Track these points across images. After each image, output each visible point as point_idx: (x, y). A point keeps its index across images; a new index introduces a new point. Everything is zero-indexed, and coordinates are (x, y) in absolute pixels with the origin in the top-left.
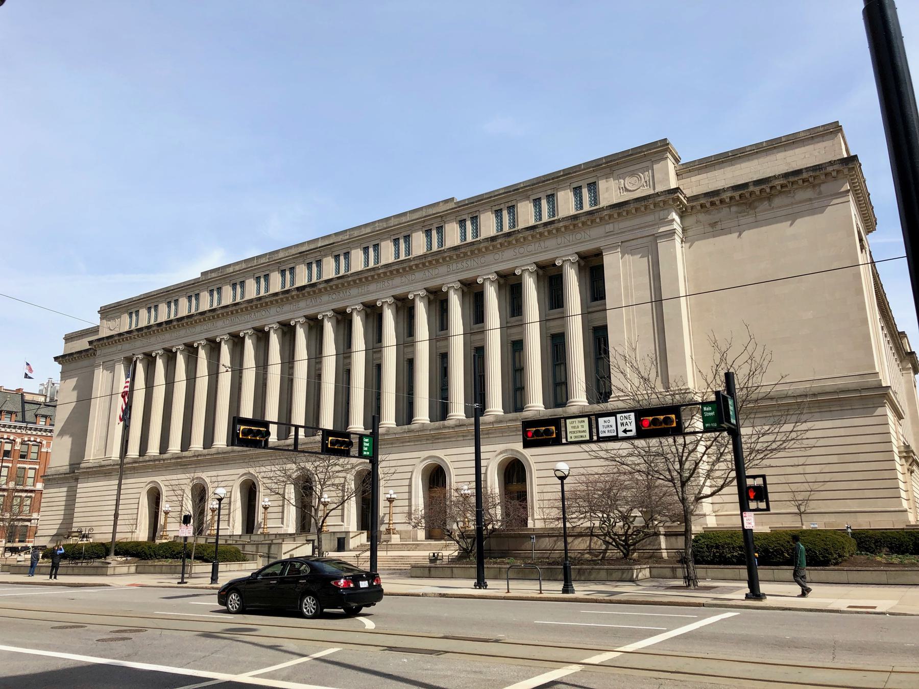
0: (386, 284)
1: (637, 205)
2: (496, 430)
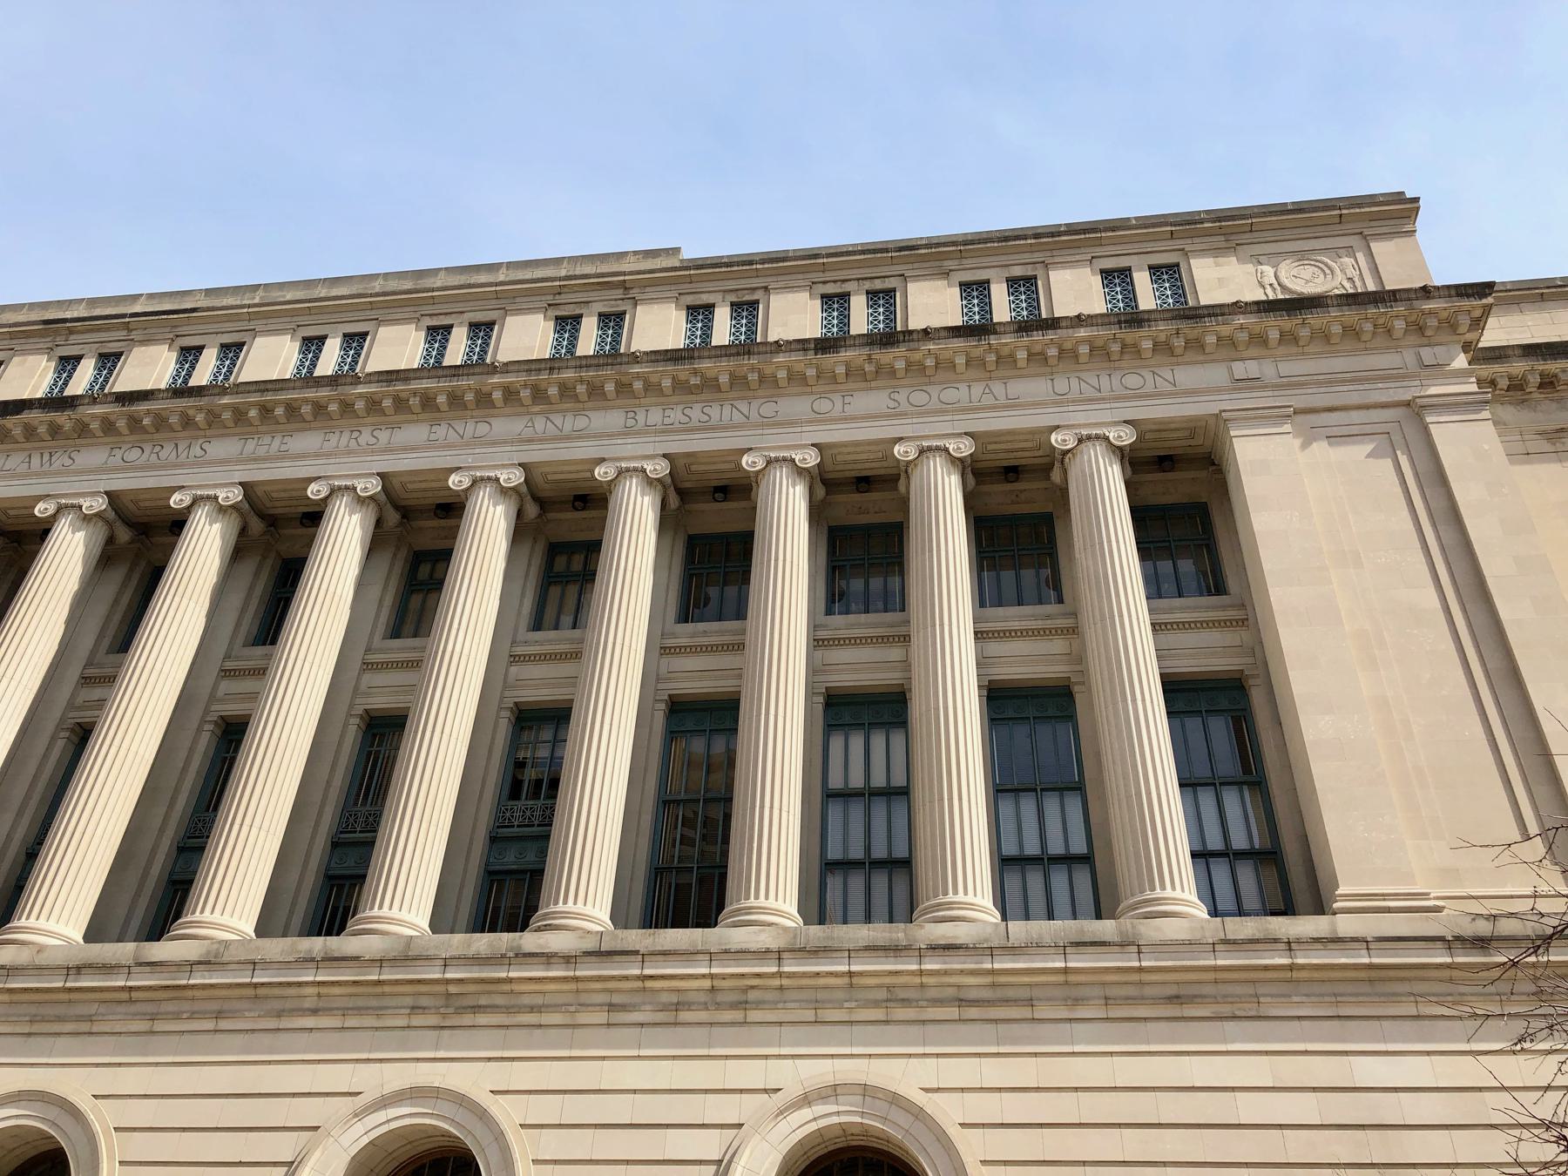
0: (366, 437)
1: (1351, 315)
2: (784, 990)
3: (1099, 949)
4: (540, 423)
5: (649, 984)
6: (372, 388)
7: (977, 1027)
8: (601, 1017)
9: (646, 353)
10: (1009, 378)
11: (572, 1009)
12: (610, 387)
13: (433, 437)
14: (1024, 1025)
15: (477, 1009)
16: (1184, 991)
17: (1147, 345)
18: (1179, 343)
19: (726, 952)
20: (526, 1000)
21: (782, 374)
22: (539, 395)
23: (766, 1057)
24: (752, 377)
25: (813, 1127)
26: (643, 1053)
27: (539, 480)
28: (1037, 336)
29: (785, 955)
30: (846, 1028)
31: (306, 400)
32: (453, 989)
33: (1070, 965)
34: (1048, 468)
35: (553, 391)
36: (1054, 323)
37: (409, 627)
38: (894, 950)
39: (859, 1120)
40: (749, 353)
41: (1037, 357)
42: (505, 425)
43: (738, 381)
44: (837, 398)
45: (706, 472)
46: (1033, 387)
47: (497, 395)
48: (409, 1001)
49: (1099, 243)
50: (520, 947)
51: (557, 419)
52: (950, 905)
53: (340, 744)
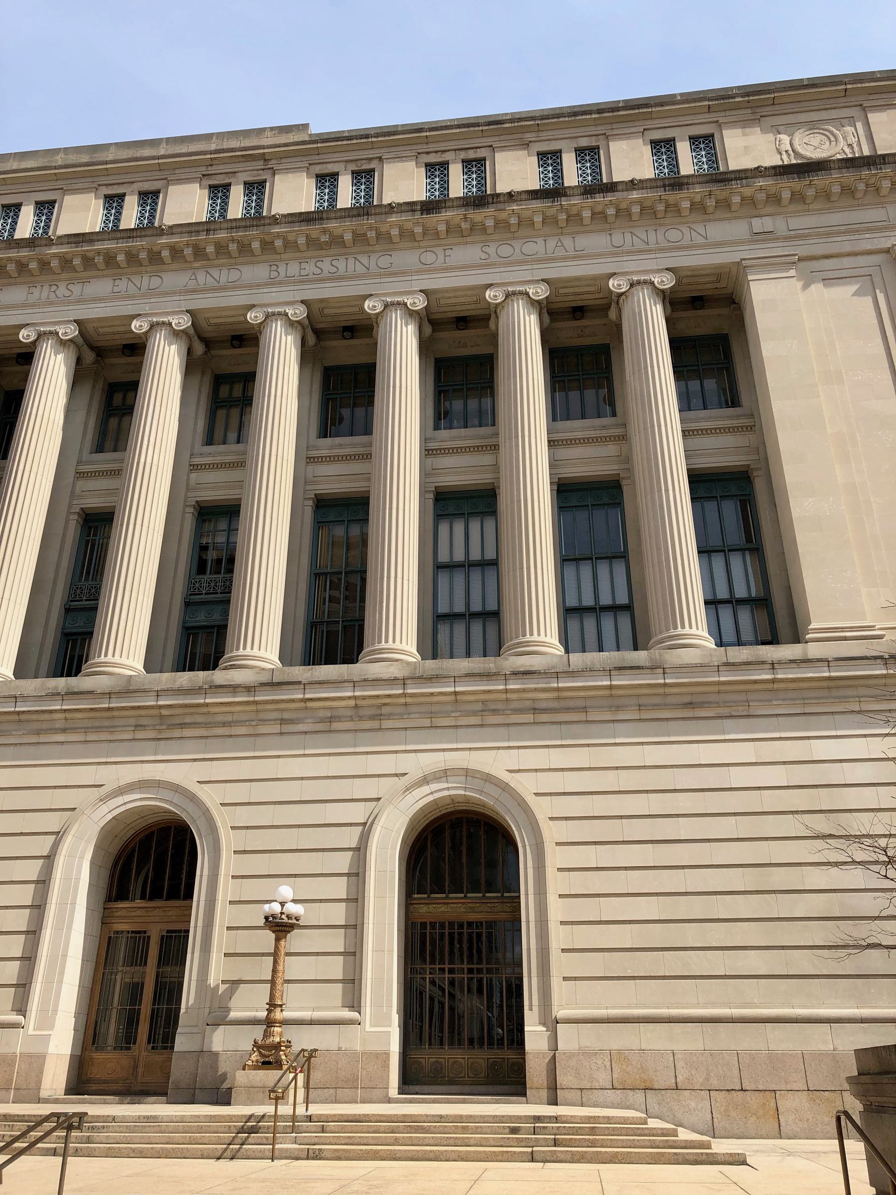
0: (62, 290)
1: (848, 176)
2: (407, 705)
3: (635, 672)
4: (201, 277)
5: (310, 704)
6: (64, 249)
7: (547, 728)
8: (276, 729)
9: (284, 216)
10: (578, 233)
11: (254, 723)
12: (256, 245)
13: (116, 289)
14: (580, 726)
15: (183, 726)
16: (695, 699)
17: (686, 204)
18: (710, 203)
19: (365, 680)
20: (220, 718)
21: (395, 232)
22: (199, 252)
23: (396, 752)
24: (371, 234)
25: (431, 798)
26: (307, 752)
27: (203, 324)
28: (599, 198)
29: (408, 682)
30: (451, 730)
31: (10, 259)
32: (164, 712)
33: (614, 683)
34: (607, 307)
35: (210, 249)
36: (612, 187)
37: (109, 444)
38: (487, 676)
39: (463, 792)
40: (368, 214)
41: (599, 216)
42: (174, 279)
43: (359, 238)
44: (440, 251)
45: (336, 315)
46: (596, 241)
47: (165, 253)
48: (132, 721)
49: (650, 117)
50: (212, 681)
51: (215, 273)
52: (527, 644)
53: (64, 536)
